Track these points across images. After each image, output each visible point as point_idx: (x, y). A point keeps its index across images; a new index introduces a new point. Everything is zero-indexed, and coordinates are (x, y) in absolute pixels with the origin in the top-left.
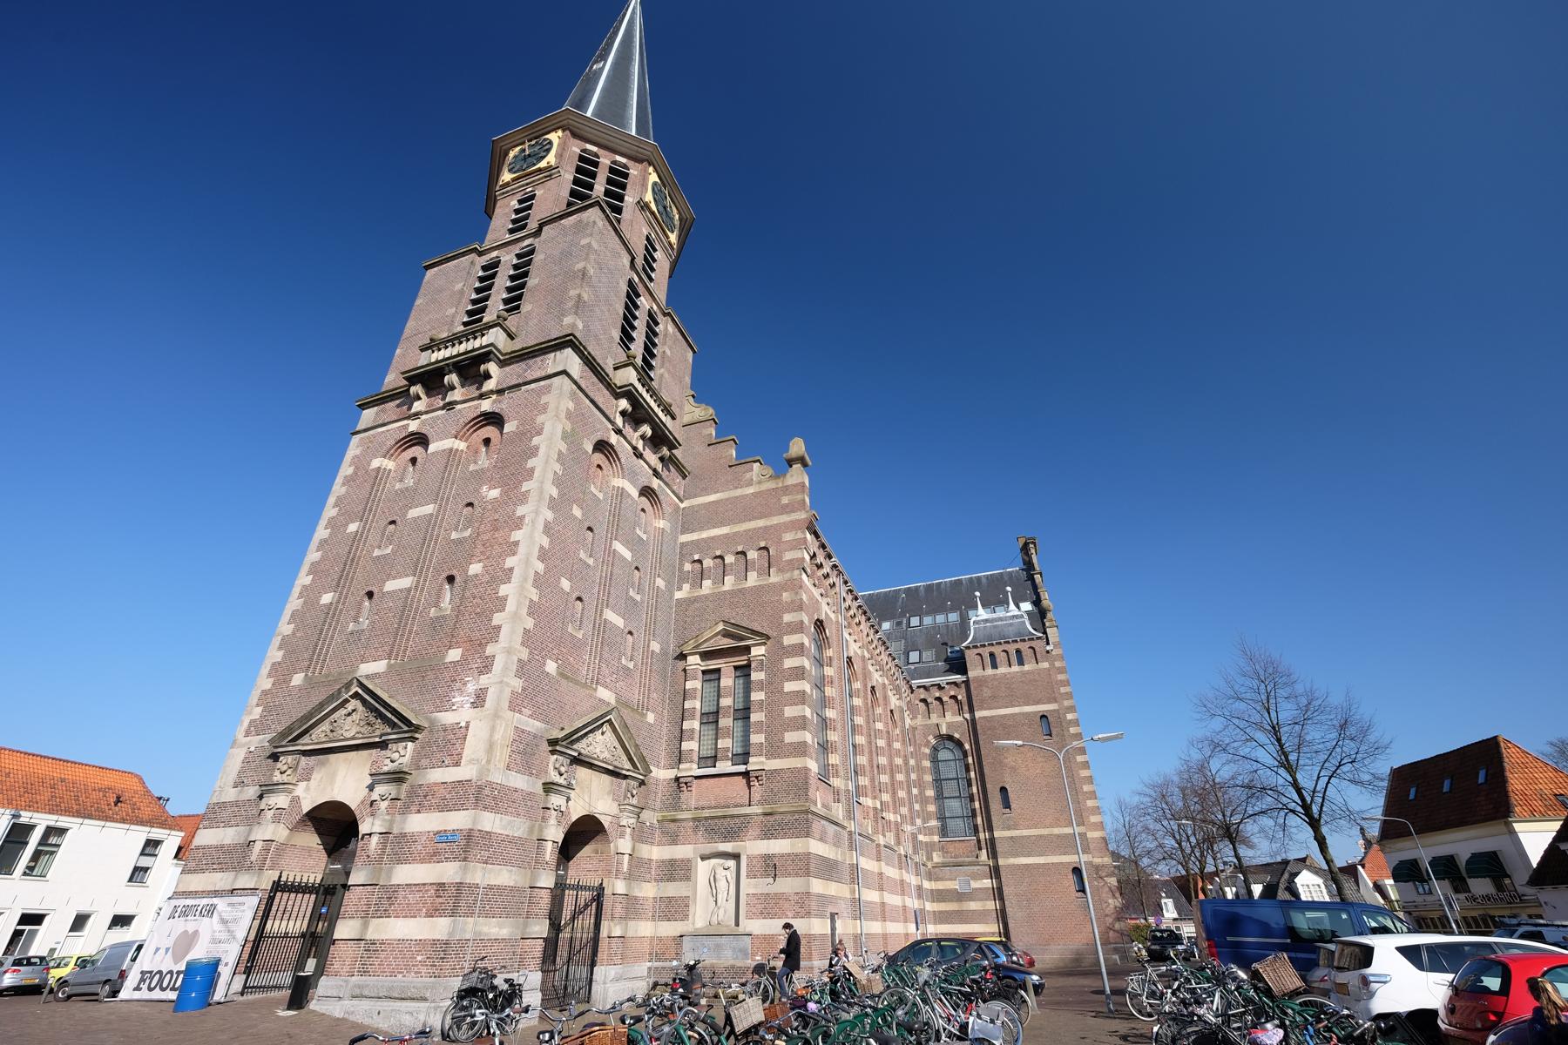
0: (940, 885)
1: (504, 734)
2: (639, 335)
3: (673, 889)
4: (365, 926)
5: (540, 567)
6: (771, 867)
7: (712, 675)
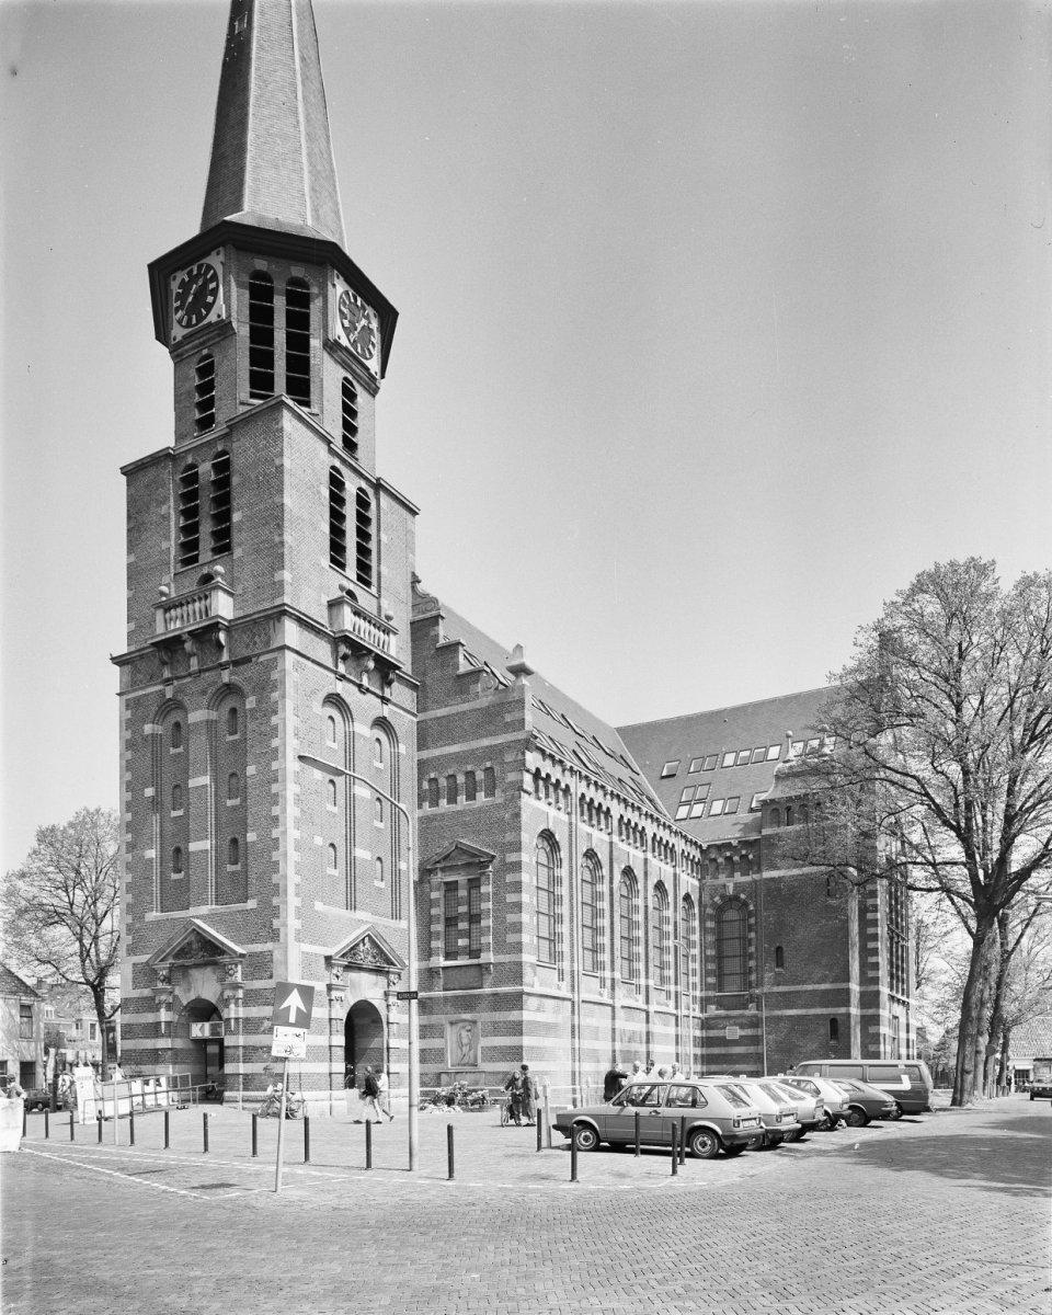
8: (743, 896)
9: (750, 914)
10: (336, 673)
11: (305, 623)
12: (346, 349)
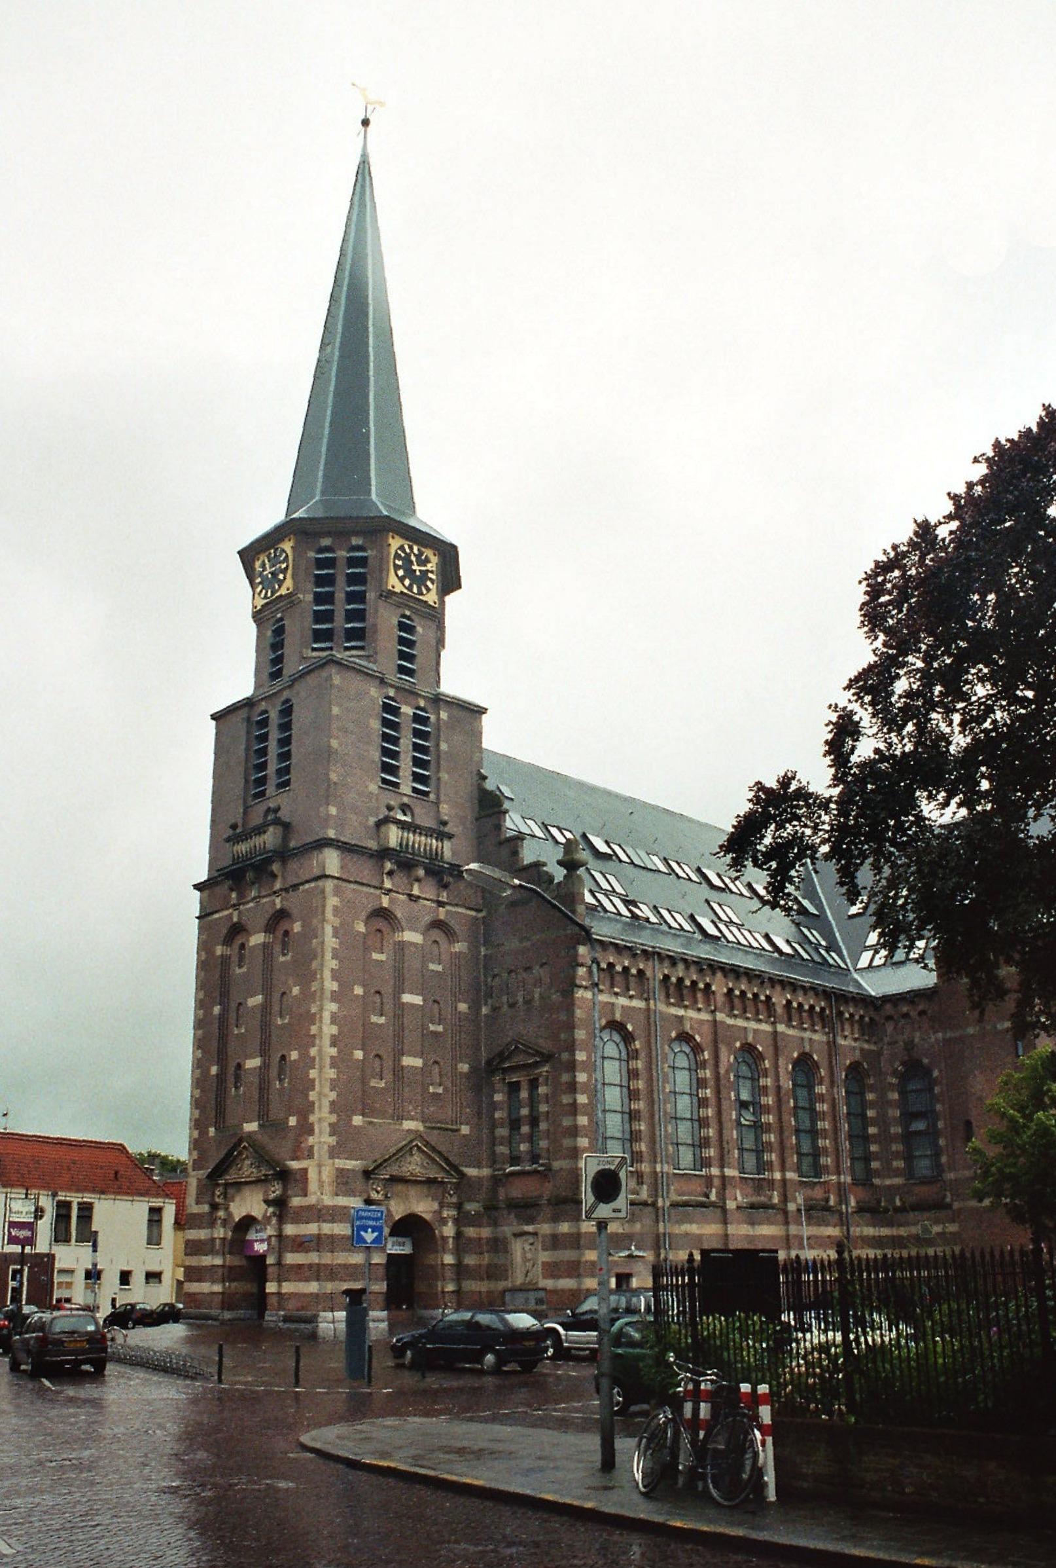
1: (327, 1174)
2: (406, 766)
3: (500, 1260)
4: (280, 1286)
5: (333, 1051)
6: (555, 1242)
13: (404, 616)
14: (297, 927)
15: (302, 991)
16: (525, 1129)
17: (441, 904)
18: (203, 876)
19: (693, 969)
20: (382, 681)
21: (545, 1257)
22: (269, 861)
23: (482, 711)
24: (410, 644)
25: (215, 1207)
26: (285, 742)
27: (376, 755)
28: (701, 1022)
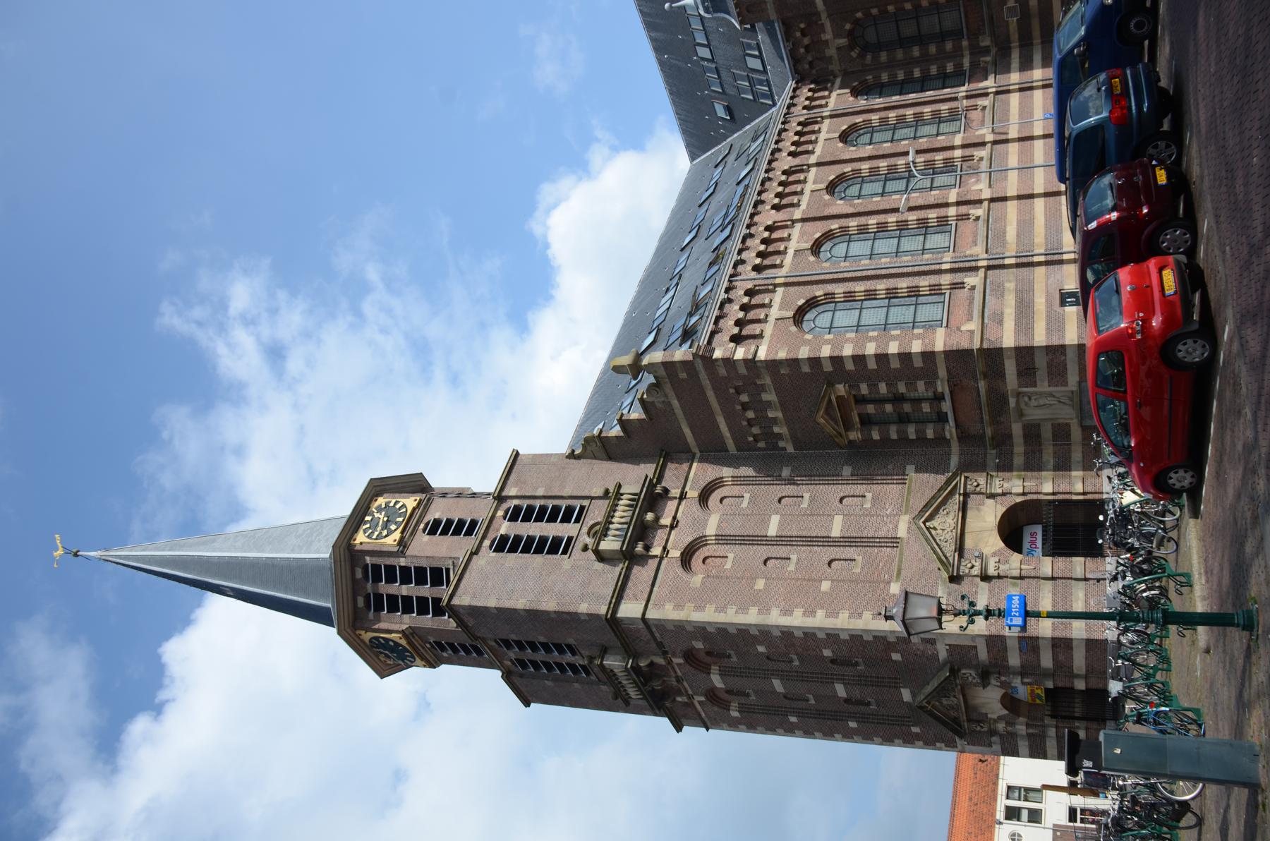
0: (1015, 36)
3: (1047, 432)
4: (1078, 676)
7: (866, 421)
8: (848, 26)
9: (867, 15)
10: (662, 558)
11: (619, 594)
12: (402, 532)
13: (424, 531)
14: (699, 645)
15: (761, 643)
16: (907, 407)
17: (682, 497)
18: (664, 723)
19: (749, 242)
20: (475, 552)
21: (1043, 386)
22: (636, 669)
23: (516, 456)
24: (449, 522)
25: (993, 732)
26: (533, 646)
27: (538, 558)
28: (802, 233)
